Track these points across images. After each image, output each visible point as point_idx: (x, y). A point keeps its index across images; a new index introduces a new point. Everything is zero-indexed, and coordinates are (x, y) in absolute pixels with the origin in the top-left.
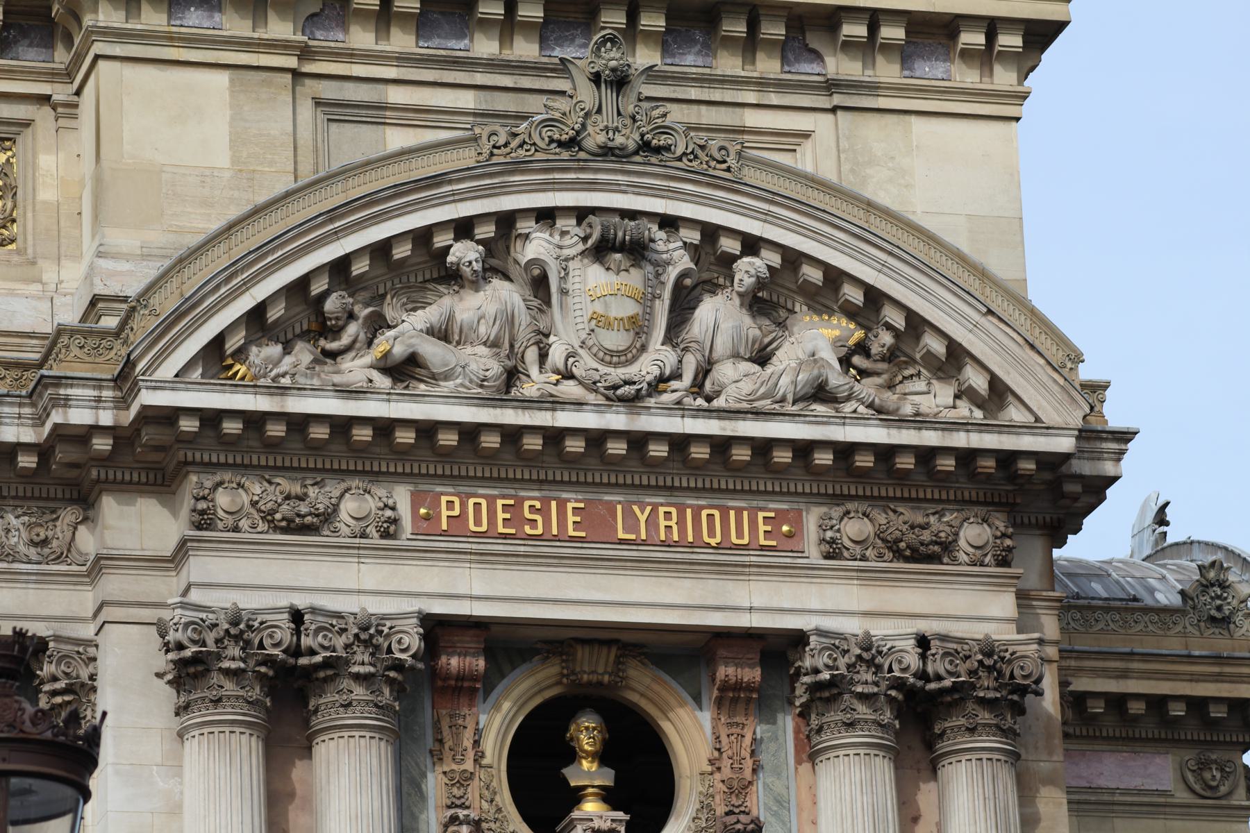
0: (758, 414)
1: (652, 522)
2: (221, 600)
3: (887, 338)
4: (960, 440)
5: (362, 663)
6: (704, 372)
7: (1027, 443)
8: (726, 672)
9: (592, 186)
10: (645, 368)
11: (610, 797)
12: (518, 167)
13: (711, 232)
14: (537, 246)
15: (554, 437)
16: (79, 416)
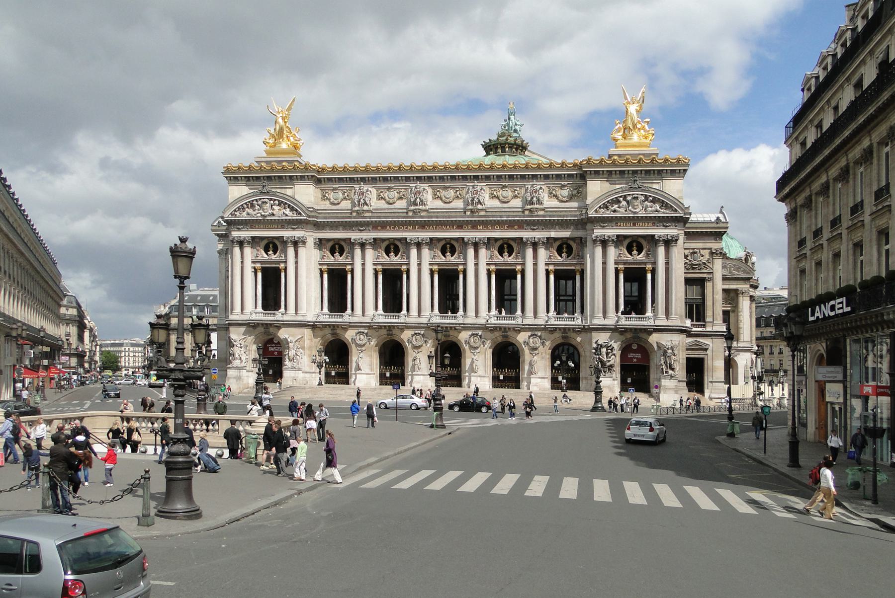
10: (637, 210)
14: (629, 198)
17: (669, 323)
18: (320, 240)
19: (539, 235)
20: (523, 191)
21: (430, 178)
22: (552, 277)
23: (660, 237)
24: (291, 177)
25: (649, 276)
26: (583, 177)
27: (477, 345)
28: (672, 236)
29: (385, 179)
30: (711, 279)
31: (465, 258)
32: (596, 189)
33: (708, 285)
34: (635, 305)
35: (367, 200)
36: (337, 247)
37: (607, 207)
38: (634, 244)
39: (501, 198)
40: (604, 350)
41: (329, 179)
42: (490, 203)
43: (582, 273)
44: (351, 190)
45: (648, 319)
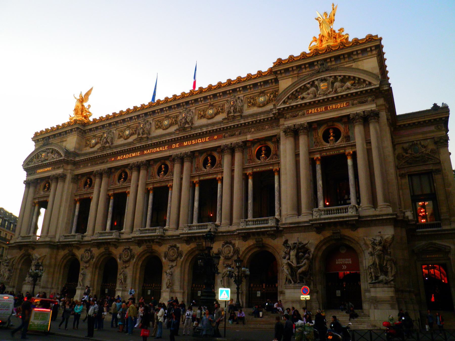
0: (341, 92)
1: (332, 107)
2: (287, 126)
3: (356, 81)
4: (365, 89)
5: (301, 128)
6: (336, 89)
7: (373, 87)
8: (344, 121)
9: (321, 75)
11: (333, 136)
12: (313, 76)
13: (335, 76)
14: (316, 83)
15: (319, 101)
16: (274, 112)
17: (377, 213)
18: (77, 175)
24: (66, 132)
25: (350, 162)
26: (276, 81)
27: (174, 258)
29: (124, 120)
32: (285, 84)
37: (296, 98)
41: (90, 130)
42: (198, 122)
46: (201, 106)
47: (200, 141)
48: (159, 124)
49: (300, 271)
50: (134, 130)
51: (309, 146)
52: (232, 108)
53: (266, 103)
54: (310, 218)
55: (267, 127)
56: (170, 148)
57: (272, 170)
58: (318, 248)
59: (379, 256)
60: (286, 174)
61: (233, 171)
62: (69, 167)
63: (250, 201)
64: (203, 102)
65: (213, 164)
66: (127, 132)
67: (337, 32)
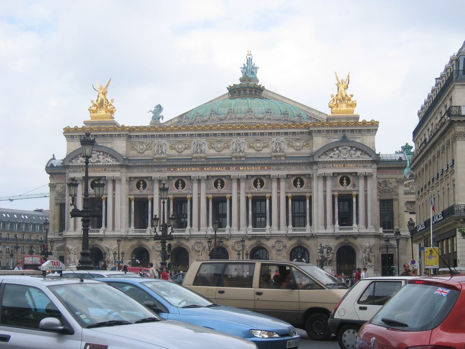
10: (346, 156)
14: (340, 149)
18: (130, 178)
19: (282, 173)
20: (270, 143)
21: (207, 135)
22: (290, 201)
23: (361, 174)
25: (354, 200)
26: (310, 133)
28: (369, 173)
29: (176, 136)
30: (397, 199)
31: (231, 190)
33: (395, 203)
34: (345, 219)
35: (163, 150)
36: (142, 183)
37: (326, 154)
38: (345, 179)
39: (256, 148)
40: (325, 250)
41: (137, 136)
43: (310, 198)
44: (152, 143)
45: (355, 229)
46: (250, 138)
47: (253, 168)
48: (212, 145)
49: (328, 260)
50: (187, 146)
51: (332, 187)
52: (278, 149)
53: (301, 147)
54: (332, 231)
55: (303, 167)
56: (228, 169)
57: (305, 196)
58: (335, 247)
59: (368, 254)
60: (317, 202)
61: (279, 193)
62: (124, 170)
63: (290, 215)
64: (252, 136)
65: (262, 185)
66: (180, 146)
67: (349, 96)
